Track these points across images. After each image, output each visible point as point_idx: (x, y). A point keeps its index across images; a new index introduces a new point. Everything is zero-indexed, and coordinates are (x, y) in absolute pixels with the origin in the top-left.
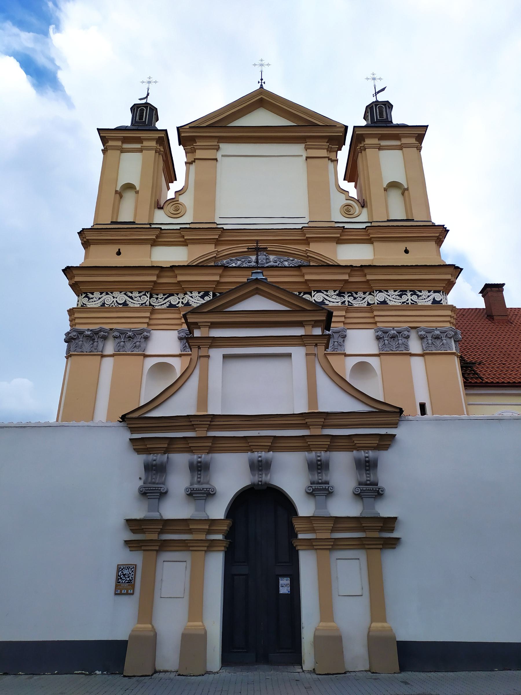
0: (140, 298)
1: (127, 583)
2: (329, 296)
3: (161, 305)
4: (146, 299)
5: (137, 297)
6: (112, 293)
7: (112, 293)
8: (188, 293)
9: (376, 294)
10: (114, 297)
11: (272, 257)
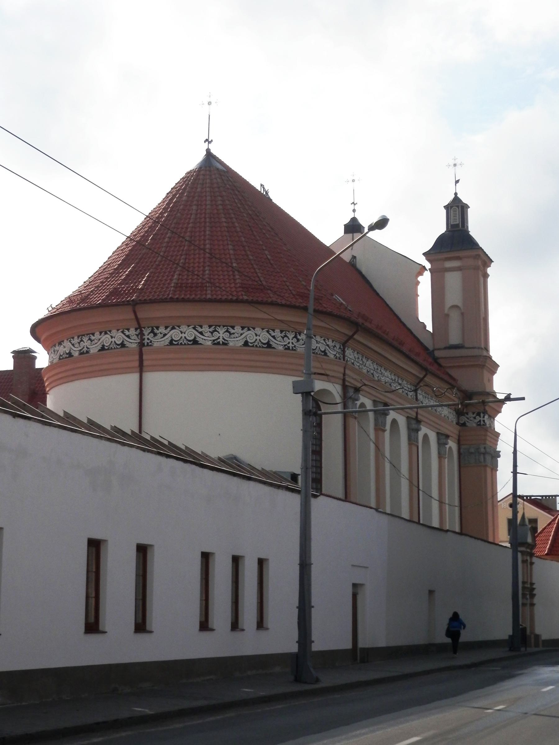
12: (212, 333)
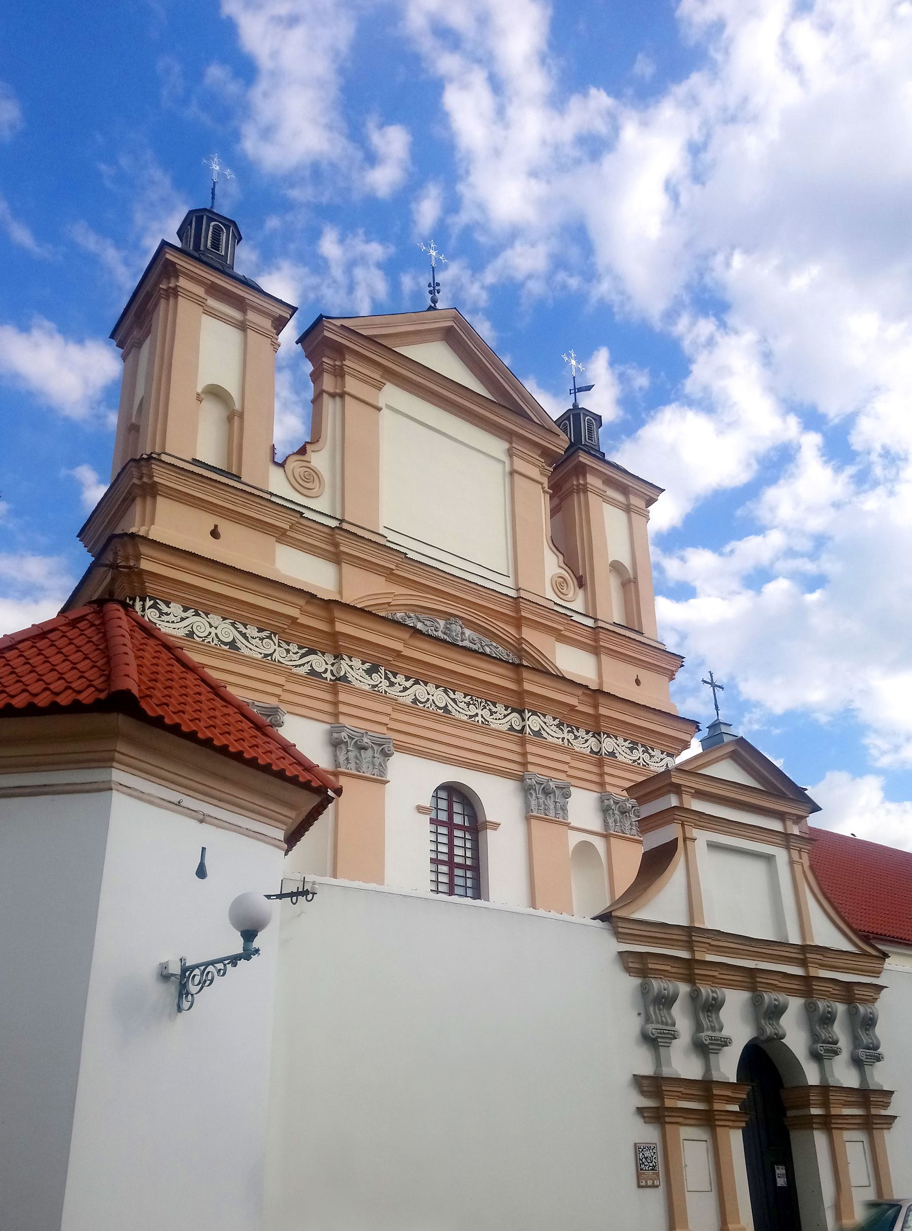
0: (262, 643)
1: (651, 1170)
2: (547, 724)
3: (296, 666)
4: (270, 646)
5: (256, 638)
6: (207, 614)
7: (207, 614)
8: (345, 657)
9: (604, 738)
10: (211, 626)
11: (468, 632)
12: (468, 704)
